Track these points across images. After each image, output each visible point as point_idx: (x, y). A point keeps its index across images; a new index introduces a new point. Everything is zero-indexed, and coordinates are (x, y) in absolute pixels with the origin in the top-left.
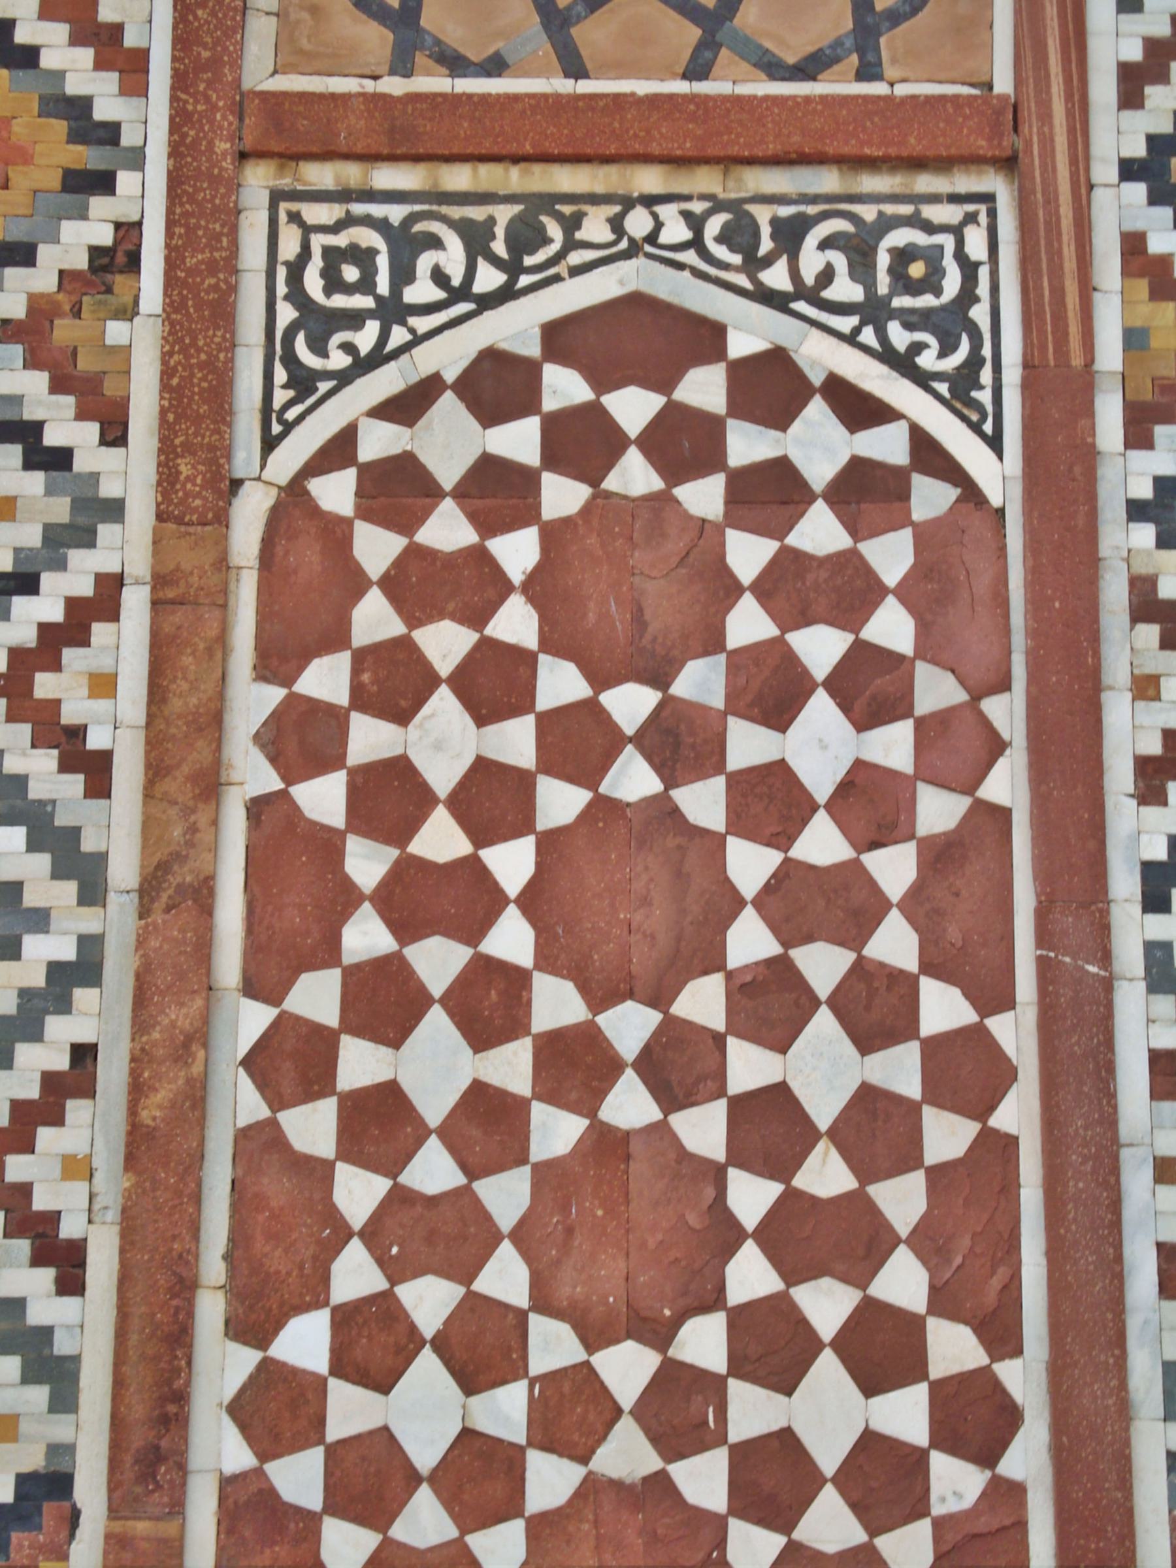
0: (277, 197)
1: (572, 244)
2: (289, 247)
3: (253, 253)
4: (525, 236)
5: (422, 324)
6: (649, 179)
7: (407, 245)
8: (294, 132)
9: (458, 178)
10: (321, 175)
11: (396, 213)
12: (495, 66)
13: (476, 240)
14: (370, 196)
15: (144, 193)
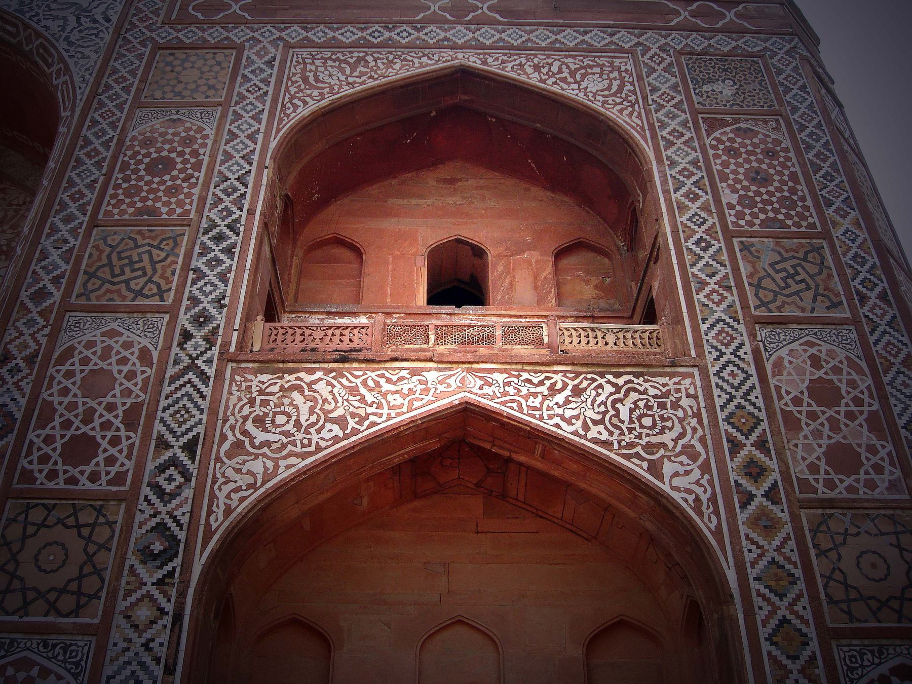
0: (838, 646)
1: (889, 654)
2: (842, 656)
3: (837, 657)
4: (881, 653)
5: (868, 669)
6: (898, 642)
7: (862, 655)
8: (839, 634)
9: (866, 642)
10: (844, 642)
11: (858, 648)
12: (866, 621)
13: (872, 652)
14: (853, 645)
15: (814, 645)
